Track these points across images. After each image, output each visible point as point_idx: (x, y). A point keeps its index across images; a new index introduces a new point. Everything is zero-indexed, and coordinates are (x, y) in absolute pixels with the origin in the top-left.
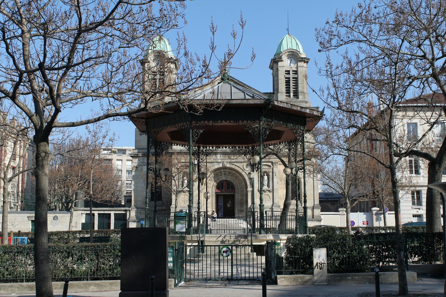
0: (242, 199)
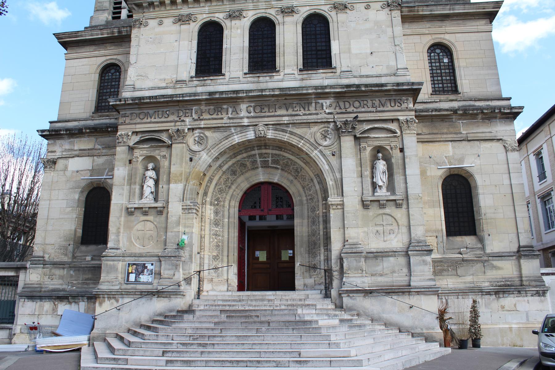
0: (313, 234)
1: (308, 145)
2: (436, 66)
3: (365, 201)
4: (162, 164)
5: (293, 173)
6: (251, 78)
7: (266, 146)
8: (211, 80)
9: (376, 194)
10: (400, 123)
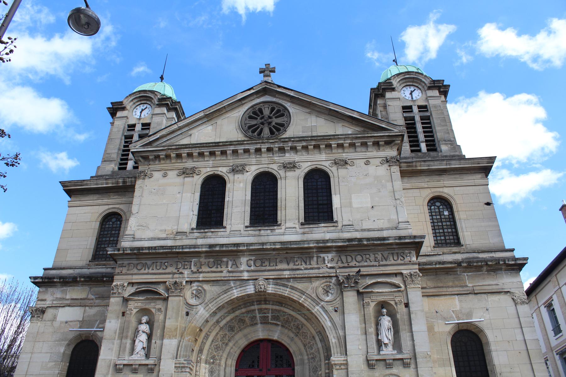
1: (309, 300)
2: (437, 219)
3: (371, 360)
4: (156, 318)
5: (294, 330)
6: (251, 231)
7: (266, 301)
8: (212, 232)
9: (381, 353)
10: (404, 277)
